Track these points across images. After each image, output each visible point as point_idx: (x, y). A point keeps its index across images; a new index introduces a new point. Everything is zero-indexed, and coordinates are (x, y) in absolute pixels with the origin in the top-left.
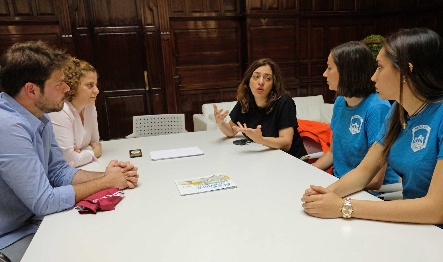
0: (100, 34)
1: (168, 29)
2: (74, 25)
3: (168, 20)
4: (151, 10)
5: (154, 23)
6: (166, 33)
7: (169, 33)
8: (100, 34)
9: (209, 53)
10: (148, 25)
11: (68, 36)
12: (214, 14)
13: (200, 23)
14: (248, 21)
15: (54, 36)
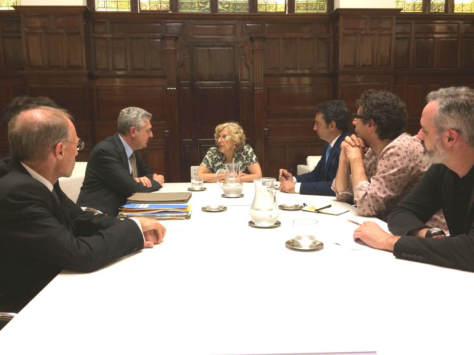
0: (201, 88)
1: (261, 85)
2: (178, 79)
3: (263, 76)
4: (247, 67)
5: (249, 79)
6: (259, 88)
7: (263, 88)
8: (201, 88)
9: (299, 108)
10: (243, 80)
11: (172, 89)
12: (307, 71)
13: (293, 80)
14: (341, 78)
15: (161, 88)
